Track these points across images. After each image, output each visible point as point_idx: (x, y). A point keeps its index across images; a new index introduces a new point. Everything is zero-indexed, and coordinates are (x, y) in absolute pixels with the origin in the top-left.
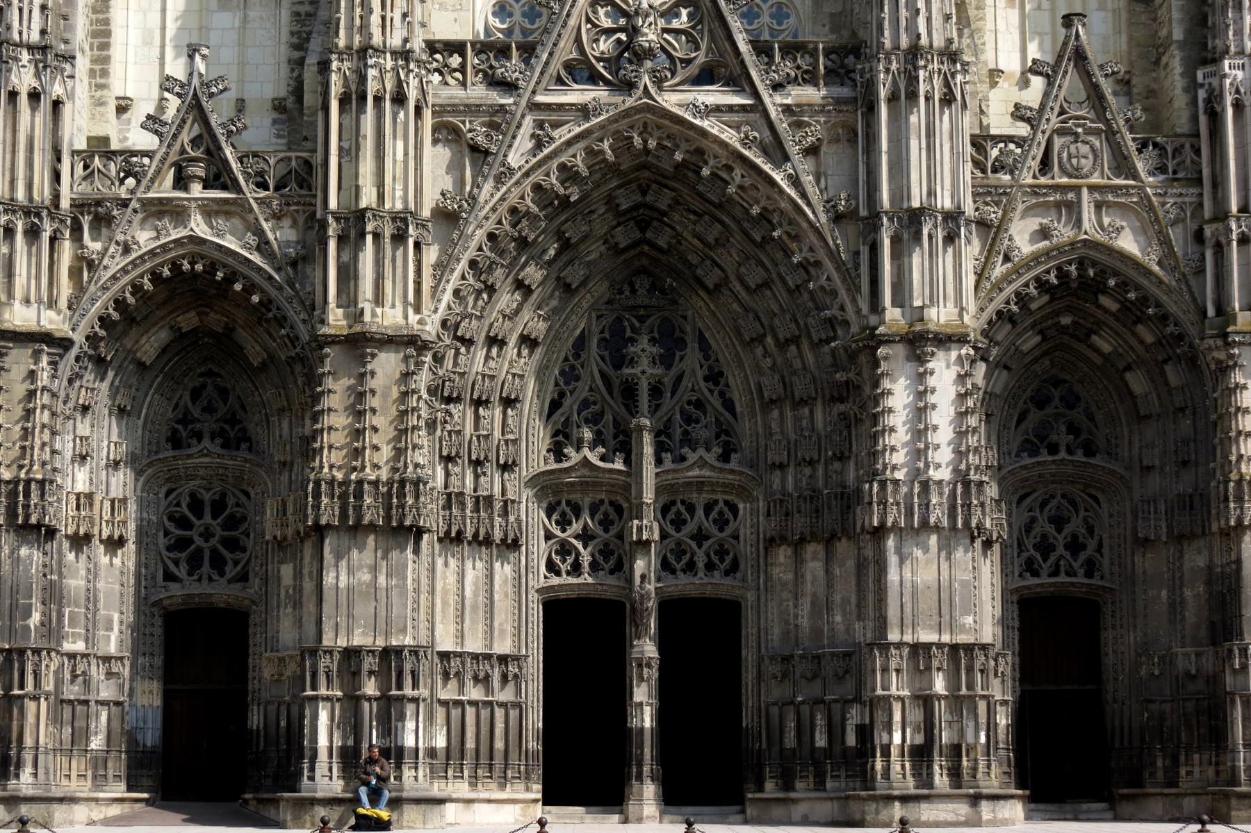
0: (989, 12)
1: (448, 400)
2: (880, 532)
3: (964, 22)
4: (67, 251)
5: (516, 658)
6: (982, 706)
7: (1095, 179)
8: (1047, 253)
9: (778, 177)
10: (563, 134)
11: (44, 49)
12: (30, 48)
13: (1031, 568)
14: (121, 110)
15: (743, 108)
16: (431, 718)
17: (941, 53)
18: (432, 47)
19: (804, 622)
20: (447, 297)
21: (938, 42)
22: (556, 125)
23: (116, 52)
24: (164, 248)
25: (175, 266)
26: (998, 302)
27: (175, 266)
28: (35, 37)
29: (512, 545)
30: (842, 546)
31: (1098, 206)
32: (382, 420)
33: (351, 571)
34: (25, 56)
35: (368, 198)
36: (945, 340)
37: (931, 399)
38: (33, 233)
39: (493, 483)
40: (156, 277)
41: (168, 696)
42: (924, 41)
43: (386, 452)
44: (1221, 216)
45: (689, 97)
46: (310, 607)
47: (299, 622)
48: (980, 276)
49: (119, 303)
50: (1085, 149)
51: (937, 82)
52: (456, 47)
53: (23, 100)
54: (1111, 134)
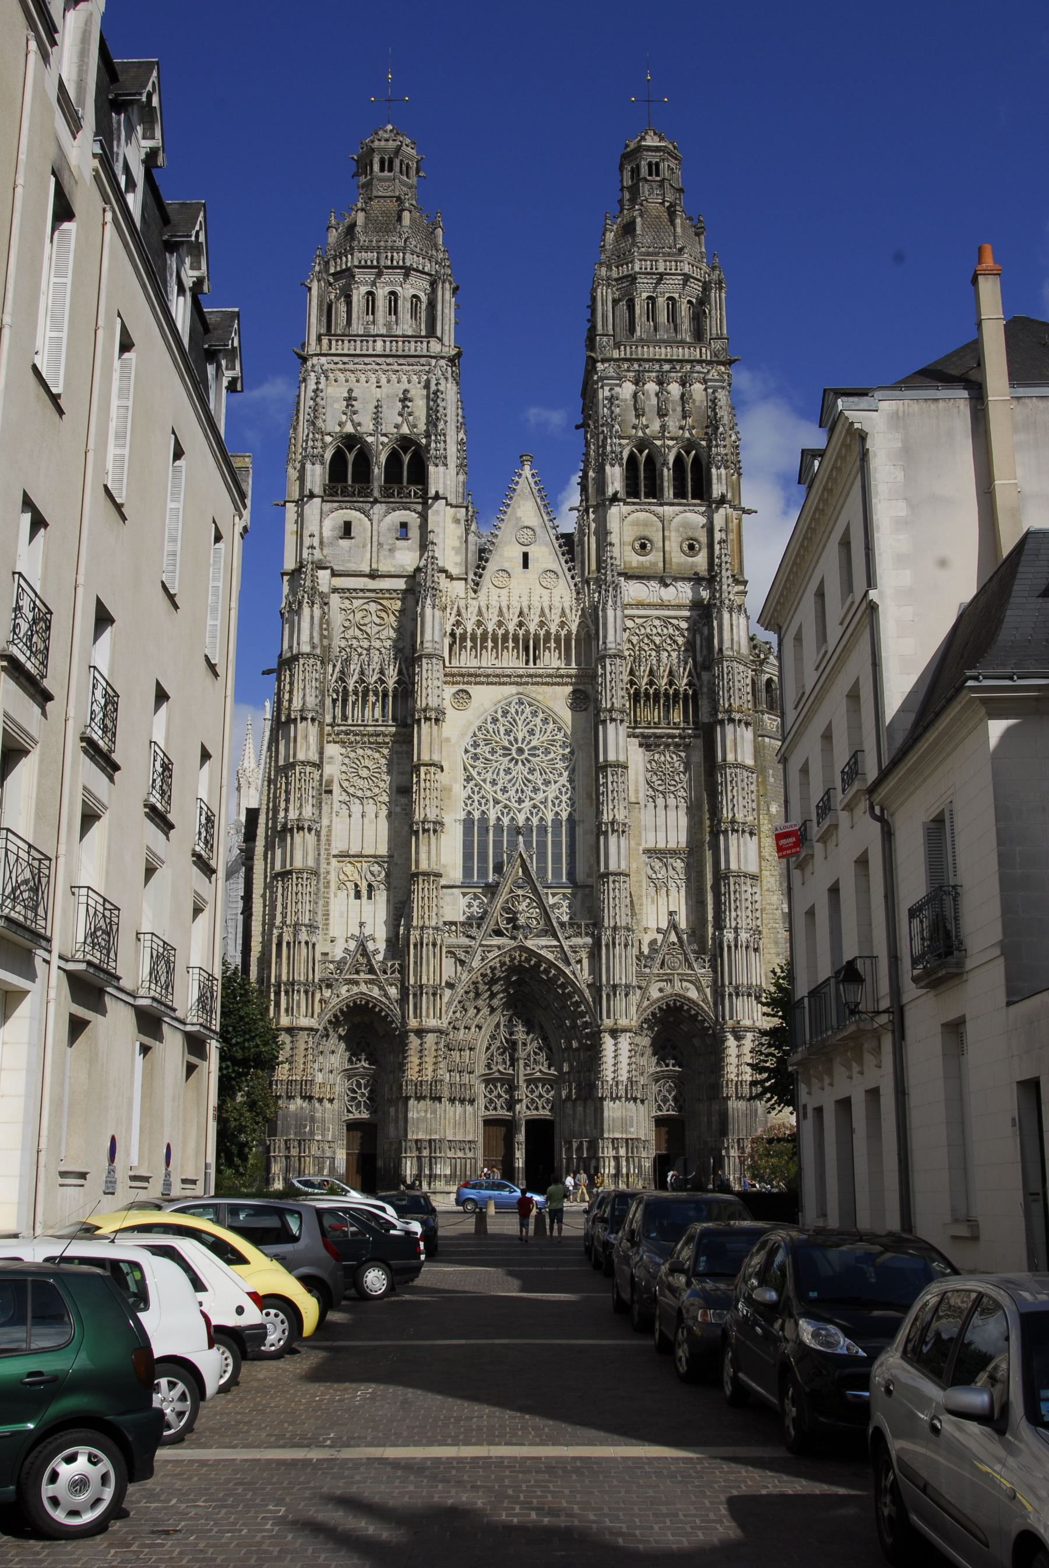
0: (645, 907)
1: (450, 1050)
2: (602, 1099)
3: (633, 914)
4: (318, 997)
5: (474, 1142)
6: (636, 1160)
7: (680, 971)
8: (662, 998)
9: (567, 971)
10: (491, 956)
11: (310, 926)
12: (306, 926)
13: (660, 1108)
14: (332, 941)
15: (555, 946)
16: (445, 1163)
17: (625, 928)
18: (445, 923)
19: (576, 1129)
20: (451, 1014)
21: (624, 924)
22: (489, 952)
23: (331, 921)
24: (351, 996)
25: (355, 1003)
26: (645, 1015)
27: (355, 1003)
28: (307, 922)
29: (472, 1102)
30: (589, 1102)
31: (681, 981)
32: (429, 1060)
33: (418, 1112)
34: (304, 928)
35: (424, 981)
36: (624, 1031)
37: (619, 1052)
38: (306, 992)
39: (466, 1078)
40: (348, 1006)
41: (348, 1154)
42: (619, 924)
43: (430, 1069)
44: (723, 985)
45: (536, 942)
46: (401, 1124)
47: (397, 1129)
48: (638, 1006)
49: (335, 1016)
50: (676, 960)
51: (623, 938)
52: (454, 923)
53: (303, 944)
54: (685, 954)
